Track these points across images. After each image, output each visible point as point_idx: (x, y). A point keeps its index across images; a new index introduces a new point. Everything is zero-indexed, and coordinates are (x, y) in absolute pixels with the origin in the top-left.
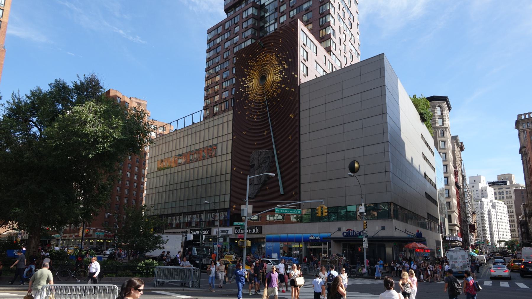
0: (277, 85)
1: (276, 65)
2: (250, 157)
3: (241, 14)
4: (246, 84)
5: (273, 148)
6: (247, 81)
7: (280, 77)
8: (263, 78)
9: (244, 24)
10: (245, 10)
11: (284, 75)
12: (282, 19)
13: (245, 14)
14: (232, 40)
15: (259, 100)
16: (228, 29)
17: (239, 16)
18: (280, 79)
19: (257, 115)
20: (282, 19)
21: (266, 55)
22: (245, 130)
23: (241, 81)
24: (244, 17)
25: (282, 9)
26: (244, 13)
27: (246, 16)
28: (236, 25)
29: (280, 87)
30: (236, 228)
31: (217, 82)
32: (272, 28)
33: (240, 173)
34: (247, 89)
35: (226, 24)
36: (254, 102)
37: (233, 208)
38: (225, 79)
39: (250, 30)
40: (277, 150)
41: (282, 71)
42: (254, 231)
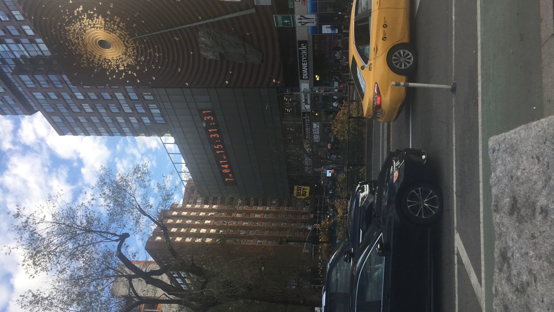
0: (110, 22)
1: (81, 25)
2: (210, 60)
3: (31, 90)
4: (114, 70)
5: (195, 27)
6: (110, 68)
7: (98, 18)
8: (103, 44)
9: (43, 86)
10: (25, 84)
11: (94, 11)
12: (30, 32)
13: (30, 84)
14: (68, 102)
15: (133, 49)
16: (54, 108)
17: (34, 94)
18: (100, 17)
19: (155, 52)
20: (30, 32)
21: (70, 40)
22: (177, 70)
23: (112, 78)
24: (34, 86)
25: (15, 33)
26: (29, 86)
27: (32, 83)
28: (47, 96)
29: (112, 19)
30: (302, 79)
31: (125, 120)
32: (44, 47)
33: (232, 74)
34: (122, 68)
35: (47, 111)
36: (137, 56)
37: (276, 83)
38: (119, 109)
39: (49, 76)
40: (198, 20)
41: (88, 14)
42: (304, 52)
